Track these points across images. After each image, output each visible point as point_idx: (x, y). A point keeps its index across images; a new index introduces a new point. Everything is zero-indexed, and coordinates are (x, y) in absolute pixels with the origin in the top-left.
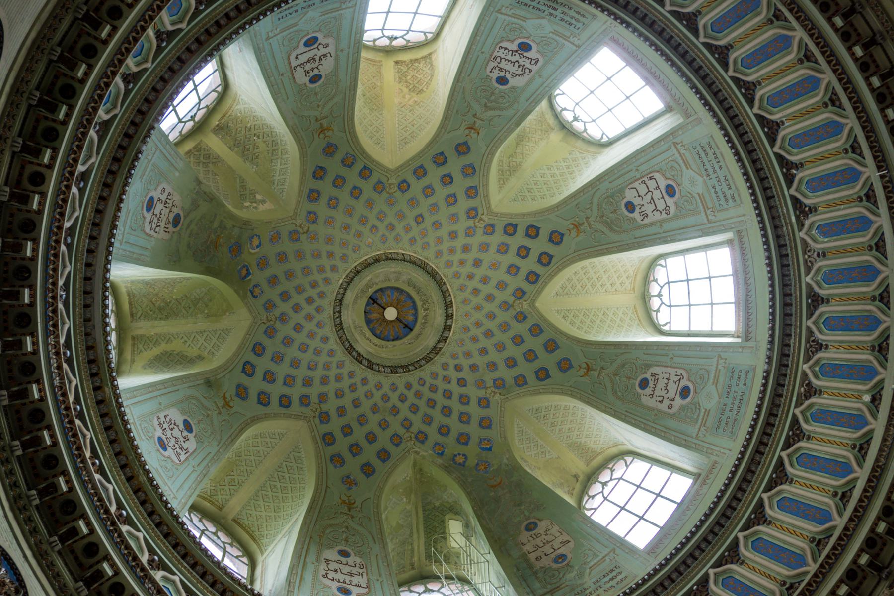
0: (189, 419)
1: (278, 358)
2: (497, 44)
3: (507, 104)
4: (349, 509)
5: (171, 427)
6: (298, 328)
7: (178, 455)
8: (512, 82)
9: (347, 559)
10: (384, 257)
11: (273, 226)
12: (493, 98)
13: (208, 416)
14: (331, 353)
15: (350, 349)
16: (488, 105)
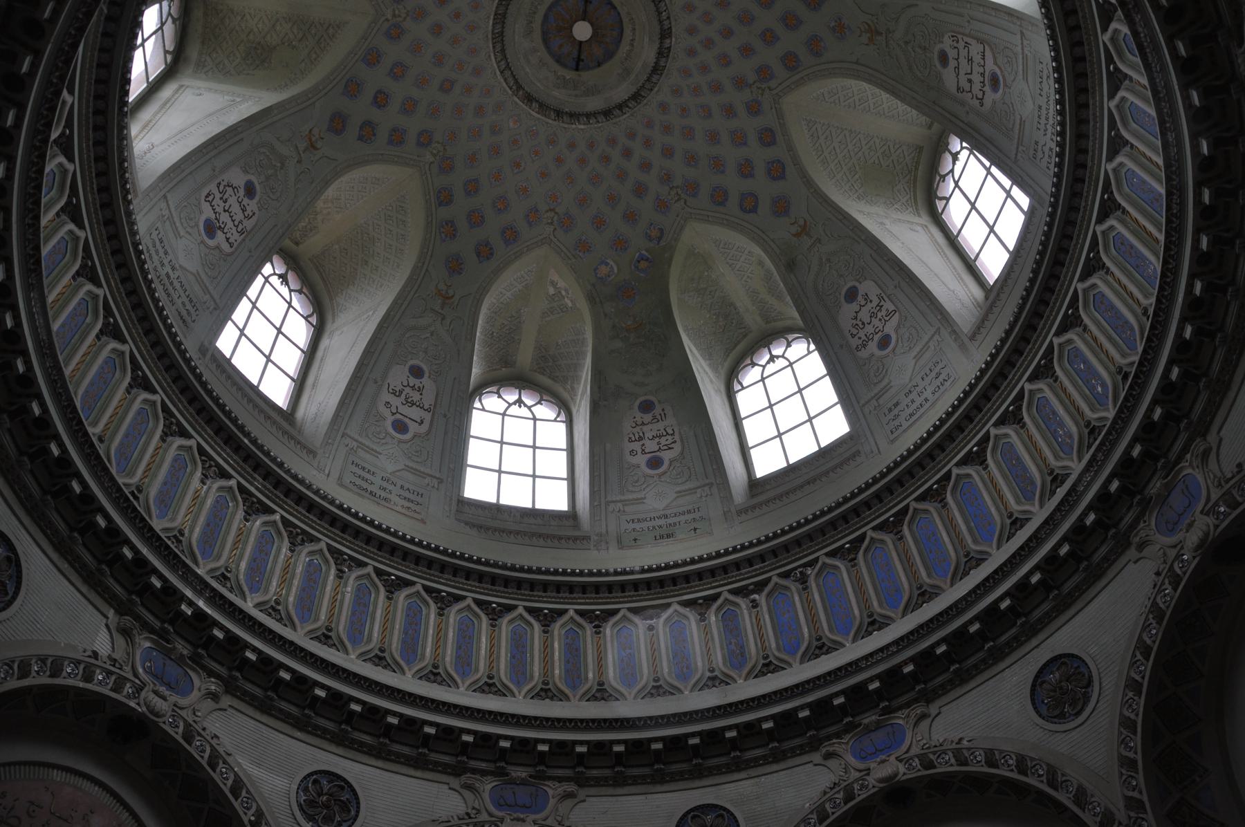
0: (843, 292)
1: (718, 165)
2: (232, 253)
3: (262, 150)
4: (880, 34)
5: (860, 323)
6: (668, 152)
7: (890, 314)
8: (238, 178)
9: (951, 59)
10: (521, 93)
11: (574, 260)
12: (270, 172)
13: (829, 260)
14: (677, 92)
15: (657, 70)
16: (279, 165)
